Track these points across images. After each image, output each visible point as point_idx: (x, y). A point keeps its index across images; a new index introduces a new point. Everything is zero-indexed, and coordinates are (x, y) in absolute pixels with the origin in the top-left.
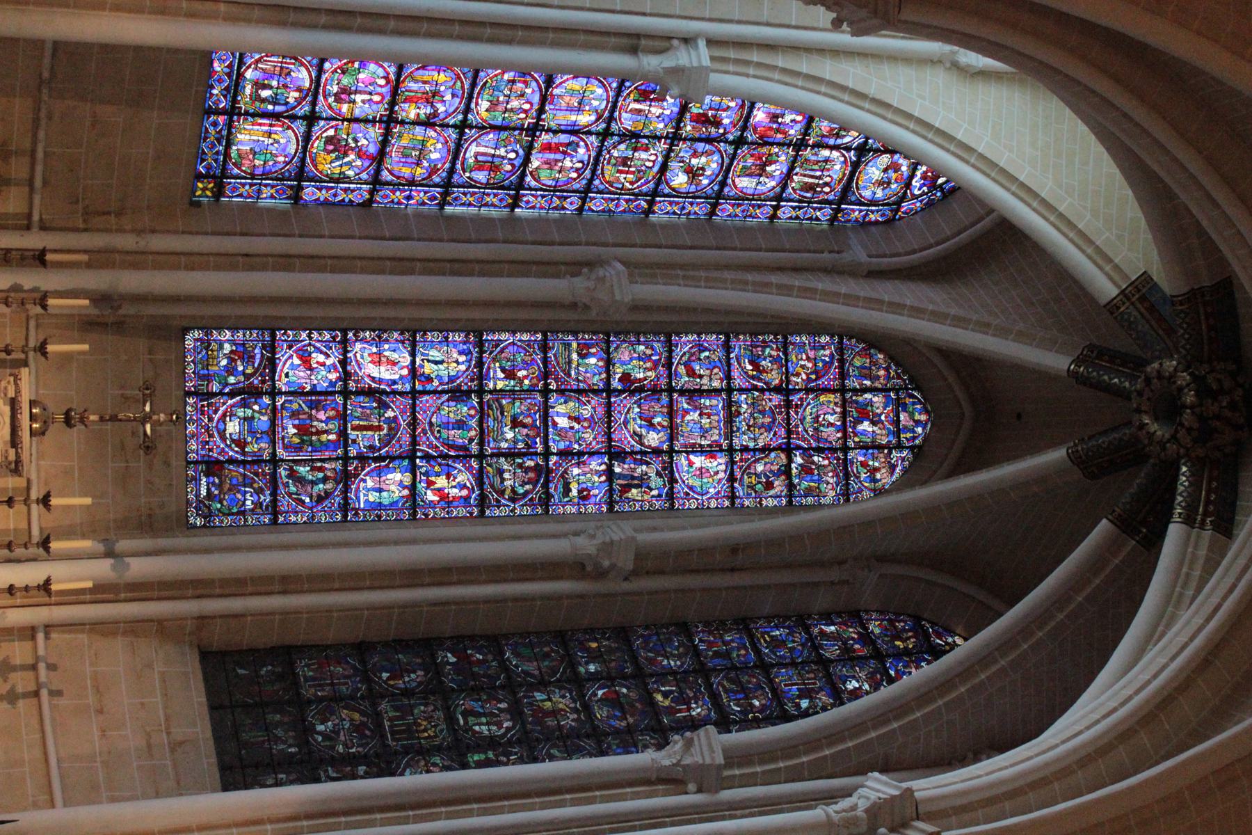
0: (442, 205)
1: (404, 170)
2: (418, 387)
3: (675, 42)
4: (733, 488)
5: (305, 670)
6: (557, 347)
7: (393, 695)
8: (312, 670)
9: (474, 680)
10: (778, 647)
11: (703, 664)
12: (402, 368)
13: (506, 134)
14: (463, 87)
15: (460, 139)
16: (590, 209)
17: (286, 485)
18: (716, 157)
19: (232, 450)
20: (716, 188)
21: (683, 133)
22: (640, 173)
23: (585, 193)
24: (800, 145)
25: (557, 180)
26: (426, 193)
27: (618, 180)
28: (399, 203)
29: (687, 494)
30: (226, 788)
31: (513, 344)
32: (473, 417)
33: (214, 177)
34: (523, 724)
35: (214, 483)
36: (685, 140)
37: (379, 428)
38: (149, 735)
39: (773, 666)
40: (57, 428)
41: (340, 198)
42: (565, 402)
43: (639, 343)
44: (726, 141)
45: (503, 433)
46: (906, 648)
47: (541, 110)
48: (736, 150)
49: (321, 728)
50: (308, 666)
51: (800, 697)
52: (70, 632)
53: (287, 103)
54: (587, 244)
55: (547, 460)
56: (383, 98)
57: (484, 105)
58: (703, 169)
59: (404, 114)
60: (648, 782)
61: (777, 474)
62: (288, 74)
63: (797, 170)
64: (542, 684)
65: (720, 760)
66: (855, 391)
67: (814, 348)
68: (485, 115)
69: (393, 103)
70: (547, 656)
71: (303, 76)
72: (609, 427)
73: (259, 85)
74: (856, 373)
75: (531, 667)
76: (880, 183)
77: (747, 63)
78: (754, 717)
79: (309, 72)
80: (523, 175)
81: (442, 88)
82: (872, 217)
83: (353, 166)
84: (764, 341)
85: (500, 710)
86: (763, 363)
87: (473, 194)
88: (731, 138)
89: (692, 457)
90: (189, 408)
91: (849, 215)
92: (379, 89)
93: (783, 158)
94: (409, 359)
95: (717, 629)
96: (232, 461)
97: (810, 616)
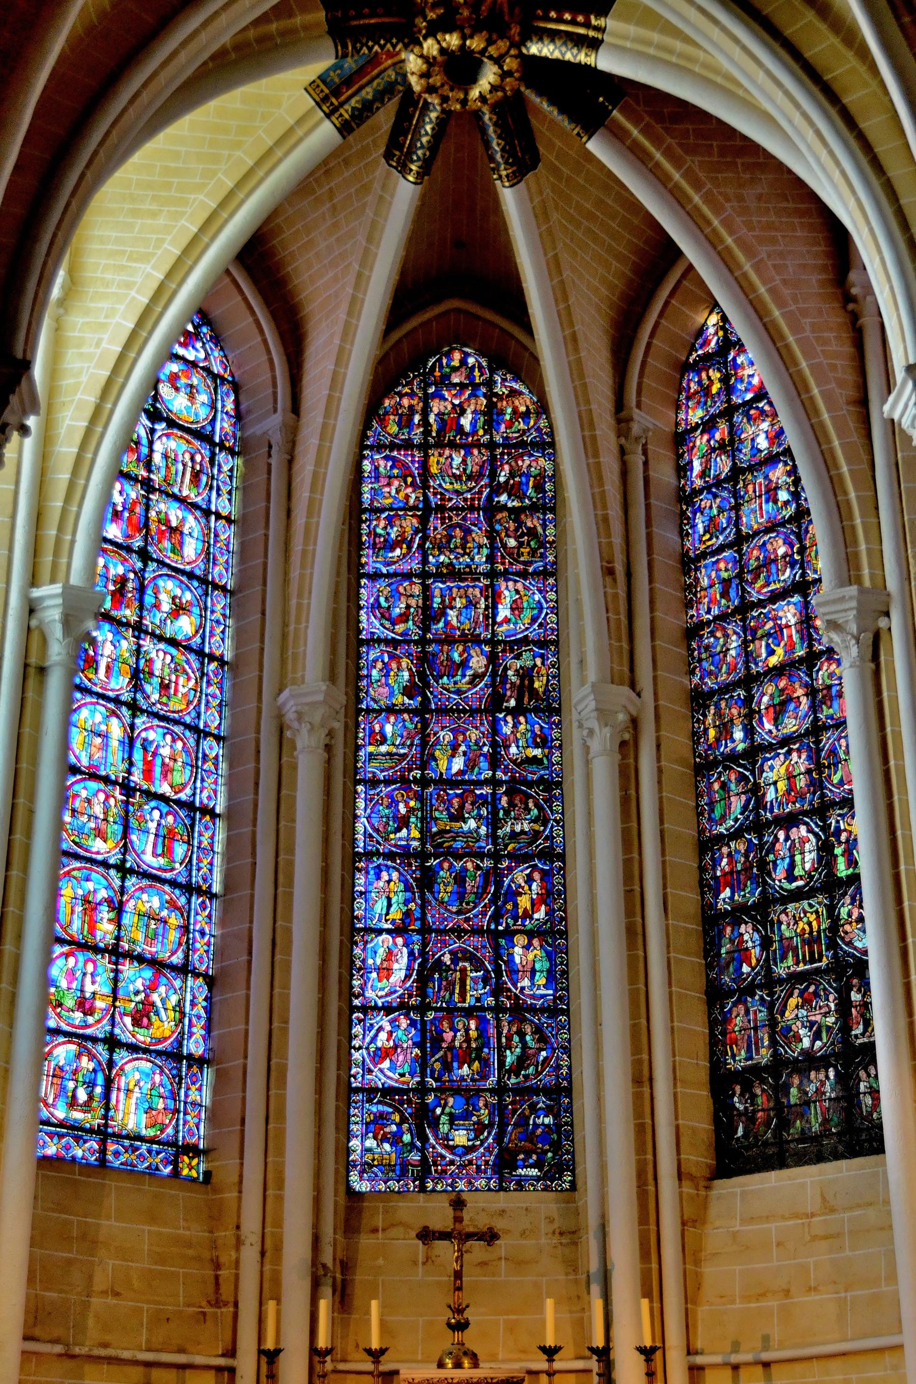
0: (212, 896)
1: (171, 938)
2: (417, 925)
3: (34, 623)
4: (536, 573)
5: (738, 1060)
6: (372, 769)
7: (767, 959)
8: (739, 1050)
9: (752, 867)
10: (716, 526)
11: (736, 611)
12: (395, 944)
13: (132, 820)
14: (79, 869)
15: (138, 873)
17: (526, 1077)
18: (160, 583)
19: (487, 1138)
20: (196, 584)
21: (134, 618)
22: (178, 670)
23: (200, 733)
24: (147, 485)
26: (197, 914)
27: (185, 695)
28: (208, 944)
29: (540, 625)
30: (881, 1150)
31: (369, 818)
32: (451, 865)
33: (176, 1156)
34: (805, 813)
35: (524, 1160)
36: (141, 617)
37: (463, 971)
38: (814, 1238)
39: (739, 531)
40: (470, 1338)
42: (436, 760)
43: (369, 676)
45: (470, 832)
46: (720, 380)
47: (106, 780)
48: (153, 560)
49: (806, 1043)
50: (734, 1056)
51: (776, 501)
52: (695, 1327)
53: (94, 1071)
54: (258, 731)
55: (500, 783)
56: (89, 960)
58: (174, 598)
59: (108, 936)
60: (877, 673)
61: (520, 523)
62: (61, 1069)
63: (176, 490)
64: (755, 792)
65: (853, 590)
66: (427, 433)
67: (377, 478)
68: (111, 844)
69: (96, 949)
70: (724, 786)
71: (64, 1052)
72: (464, 711)
73: (73, 1103)
74: (405, 431)
75: (737, 804)
76: (192, 397)
77: (58, 541)
78: (798, 553)
79: (59, 1044)
80: (178, 802)
81: (80, 892)
82: (230, 407)
83: (165, 996)
84: (369, 535)
85: (787, 838)
86: (393, 536)
87: (199, 860)
88: (139, 565)
89: (499, 619)
90: (439, 1188)
91: (226, 434)
93: (162, 506)
94: (385, 936)
95: (695, 594)
96: (499, 1139)
97: (683, 489)
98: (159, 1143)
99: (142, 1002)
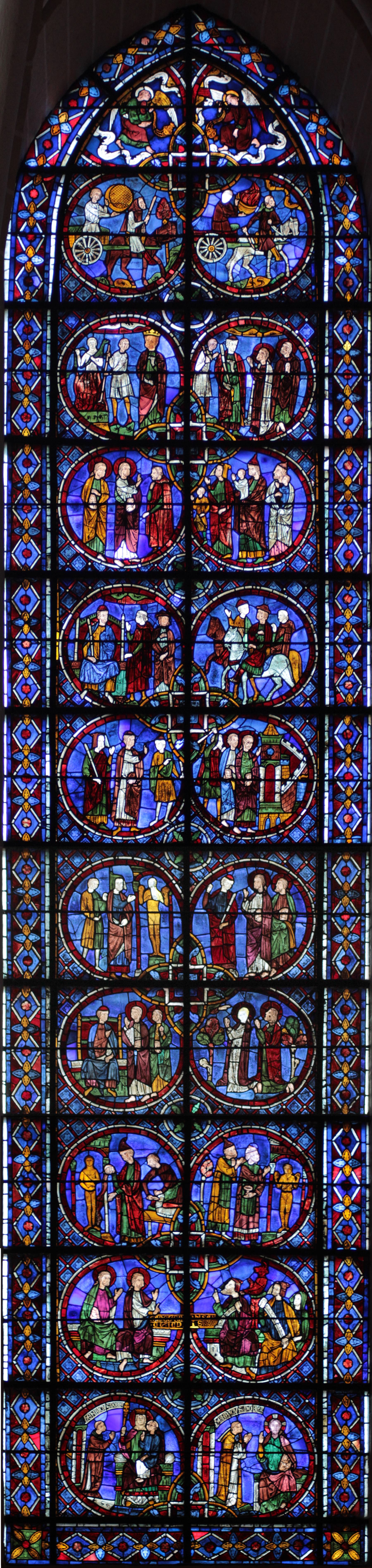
14: (103, 1135)
16: (359, 831)
25: (293, 916)
26: (335, 1156)
41: (355, 1312)
44: (187, 603)
47: (145, 984)
57: (138, 1089)
69: (147, 1251)
80: (288, 984)
81: (109, 1169)
92: (121, 1281)
98: (284, 1520)
99: (237, 1316)
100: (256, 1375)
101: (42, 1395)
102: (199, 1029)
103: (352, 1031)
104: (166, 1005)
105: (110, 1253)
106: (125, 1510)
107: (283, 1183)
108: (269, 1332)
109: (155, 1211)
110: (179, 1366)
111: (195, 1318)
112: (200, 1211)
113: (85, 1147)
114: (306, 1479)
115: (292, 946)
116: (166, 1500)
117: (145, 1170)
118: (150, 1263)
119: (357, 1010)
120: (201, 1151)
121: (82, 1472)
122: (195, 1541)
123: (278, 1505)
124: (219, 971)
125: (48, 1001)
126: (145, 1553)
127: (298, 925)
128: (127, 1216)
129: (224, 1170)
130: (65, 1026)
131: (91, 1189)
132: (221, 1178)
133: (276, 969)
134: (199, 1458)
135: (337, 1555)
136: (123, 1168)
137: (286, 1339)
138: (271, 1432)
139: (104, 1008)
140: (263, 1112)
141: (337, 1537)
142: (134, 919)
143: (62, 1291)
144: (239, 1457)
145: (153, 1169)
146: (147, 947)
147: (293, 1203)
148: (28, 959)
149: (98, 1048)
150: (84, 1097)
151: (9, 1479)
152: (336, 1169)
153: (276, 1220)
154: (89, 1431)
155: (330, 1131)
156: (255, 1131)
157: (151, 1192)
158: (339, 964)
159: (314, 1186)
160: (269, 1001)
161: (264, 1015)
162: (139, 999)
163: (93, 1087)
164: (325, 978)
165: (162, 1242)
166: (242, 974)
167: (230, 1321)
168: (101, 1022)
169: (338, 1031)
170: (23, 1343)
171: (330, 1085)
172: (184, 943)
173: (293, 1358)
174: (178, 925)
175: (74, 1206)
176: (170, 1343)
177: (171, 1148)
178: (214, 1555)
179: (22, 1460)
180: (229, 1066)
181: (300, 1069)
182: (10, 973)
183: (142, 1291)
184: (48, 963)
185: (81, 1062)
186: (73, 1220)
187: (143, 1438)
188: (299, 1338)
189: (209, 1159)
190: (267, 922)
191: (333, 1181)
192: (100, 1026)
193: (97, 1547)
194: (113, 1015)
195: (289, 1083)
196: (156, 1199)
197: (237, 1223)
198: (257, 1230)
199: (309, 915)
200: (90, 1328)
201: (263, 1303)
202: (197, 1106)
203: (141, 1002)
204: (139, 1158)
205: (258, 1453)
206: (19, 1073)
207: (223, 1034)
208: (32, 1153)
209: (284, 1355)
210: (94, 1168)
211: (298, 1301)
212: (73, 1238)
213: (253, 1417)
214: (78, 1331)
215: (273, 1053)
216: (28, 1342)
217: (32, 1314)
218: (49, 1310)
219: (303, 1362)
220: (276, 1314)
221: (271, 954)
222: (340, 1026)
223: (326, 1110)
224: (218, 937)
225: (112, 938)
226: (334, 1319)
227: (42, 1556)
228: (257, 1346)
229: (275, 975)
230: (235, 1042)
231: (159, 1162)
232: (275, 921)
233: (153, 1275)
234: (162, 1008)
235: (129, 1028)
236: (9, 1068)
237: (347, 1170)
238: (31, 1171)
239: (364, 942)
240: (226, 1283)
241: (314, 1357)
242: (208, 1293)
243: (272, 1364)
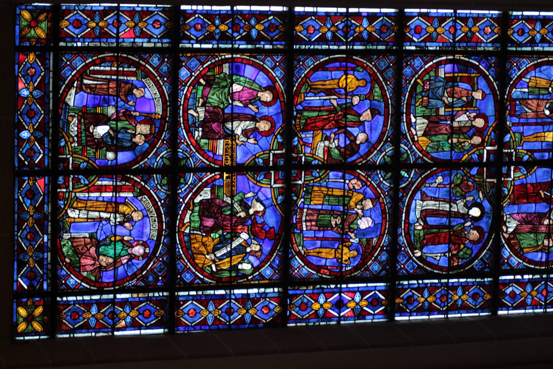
14: (384, 95)
26: (363, 293)
41: (236, 317)
47: (501, 129)
57: (421, 124)
69: (289, 133)
80: (497, 248)
81: (356, 100)
92: (265, 110)
99: (234, 214)
100: (183, 232)
101: (168, 40)
102: (466, 175)
103: (460, 303)
104: (485, 147)
105: (288, 100)
106: (65, 116)
107: (342, 250)
108: (220, 242)
109: (322, 140)
110: (192, 163)
111: (232, 176)
112: (321, 179)
113: (374, 80)
114: (91, 280)
115: (525, 250)
116: (73, 152)
117: (355, 131)
118: (279, 137)
119: (475, 306)
120: (369, 179)
121: (99, 76)
122: (36, 180)
123: (68, 255)
124: (509, 191)
125: (491, 49)
126: (25, 134)
127: (540, 254)
128: (318, 116)
129: (354, 199)
130: (472, 63)
131: (341, 84)
132: (348, 196)
133: (508, 237)
134: (111, 183)
135: (22, 312)
136: (356, 112)
137: (212, 257)
138: (133, 247)
139: (484, 95)
140: (399, 231)
141: (39, 310)
142: (549, 120)
143: (256, 59)
144: (112, 219)
145: (356, 138)
146: (529, 131)
147: (326, 259)
148: (522, 32)
149: (454, 90)
150: (416, 79)
151: (94, 9)
152: (353, 294)
153: (313, 245)
154: (136, 83)
155: (383, 288)
156: (384, 224)
157: (337, 136)
158: (511, 289)
159: (340, 277)
160: (485, 232)
161: (474, 229)
162: (490, 125)
163: (423, 87)
164: (500, 278)
165: (296, 146)
166: (505, 210)
167: (229, 207)
168: (474, 93)
169: (460, 292)
170: (213, 23)
171: (418, 286)
172: (530, 161)
173: (197, 265)
174: (543, 157)
175: (327, 70)
176: (211, 155)
177: (372, 153)
178: (23, 198)
179: (110, 21)
180: (436, 201)
181: (431, 260)
182: (513, 18)
183: (256, 129)
184: (519, 49)
185: (443, 76)
186: (315, 69)
187: (129, 131)
188: (214, 269)
189: (363, 186)
190: (543, 229)
191: (343, 293)
192: (470, 92)
193: (31, 90)
194: (478, 103)
195: (422, 252)
196: (332, 141)
197: (311, 212)
198: (305, 229)
199: (547, 263)
200: (224, 84)
201: (244, 236)
202: (406, 175)
203: (488, 126)
204: (364, 126)
205: (115, 235)
206: (436, 24)
207: (461, 195)
208: (370, 34)
209: (200, 256)
210: (357, 87)
211: (246, 267)
212: (301, 69)
213: (147, 230)
214: (222, 72)
215: (445, 237)
216: (213, 28)
217: (238, 32)
218: (241, 47)
219: (194, 273)
220: (235, 248)
221: (520, 233)
222: (464, 293)
223: (399, 284)
224: (534, 190)
225: (535, 102)
226: (230, 299)
227: (23, 38)
228: (208, 231)
229: (504, 237)
230: (454, 205)
231: (361, 143)
232: (544, 235)
233: (269, 138)
234: (482, 144)
235: (468, 117)
236: (440, 15)
237: (352, 305)
238: (356, 32)
239: (525, 309)
240: (261, 203)
241: (198, 283)
242: (253, 187)
243: (192, 246)
